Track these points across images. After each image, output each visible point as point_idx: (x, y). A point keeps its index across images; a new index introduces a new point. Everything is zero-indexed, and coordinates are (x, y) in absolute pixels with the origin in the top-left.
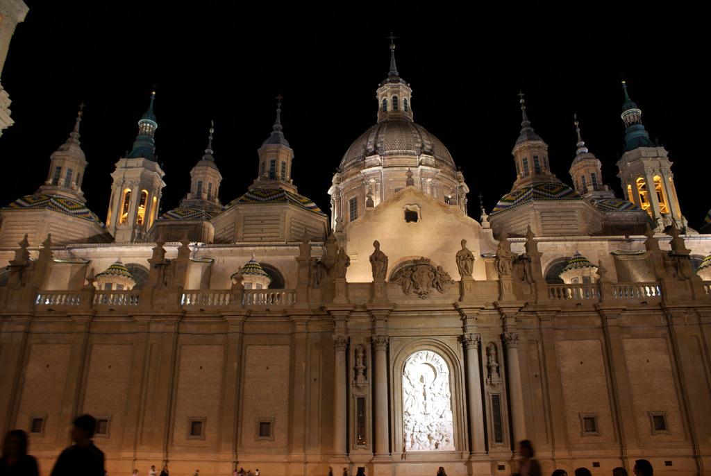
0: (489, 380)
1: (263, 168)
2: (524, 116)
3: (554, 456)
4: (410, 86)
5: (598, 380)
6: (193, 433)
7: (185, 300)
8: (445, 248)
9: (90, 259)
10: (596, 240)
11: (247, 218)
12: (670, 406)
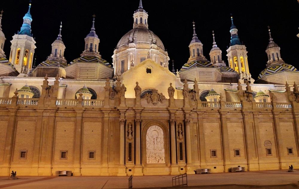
0: (178, 137)
1: (87, 46)
2: (194, 32)
3: (259, 162)
4: (148, 14)
5: (218, 137)
6: (62, 157)
7: (58, 103)
8: (162, 85)
9: (11, 83)
10: (219, 84)
11: (81, 68)
12: (241, 147)
